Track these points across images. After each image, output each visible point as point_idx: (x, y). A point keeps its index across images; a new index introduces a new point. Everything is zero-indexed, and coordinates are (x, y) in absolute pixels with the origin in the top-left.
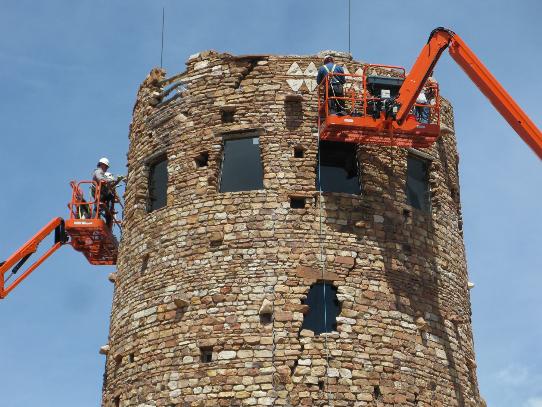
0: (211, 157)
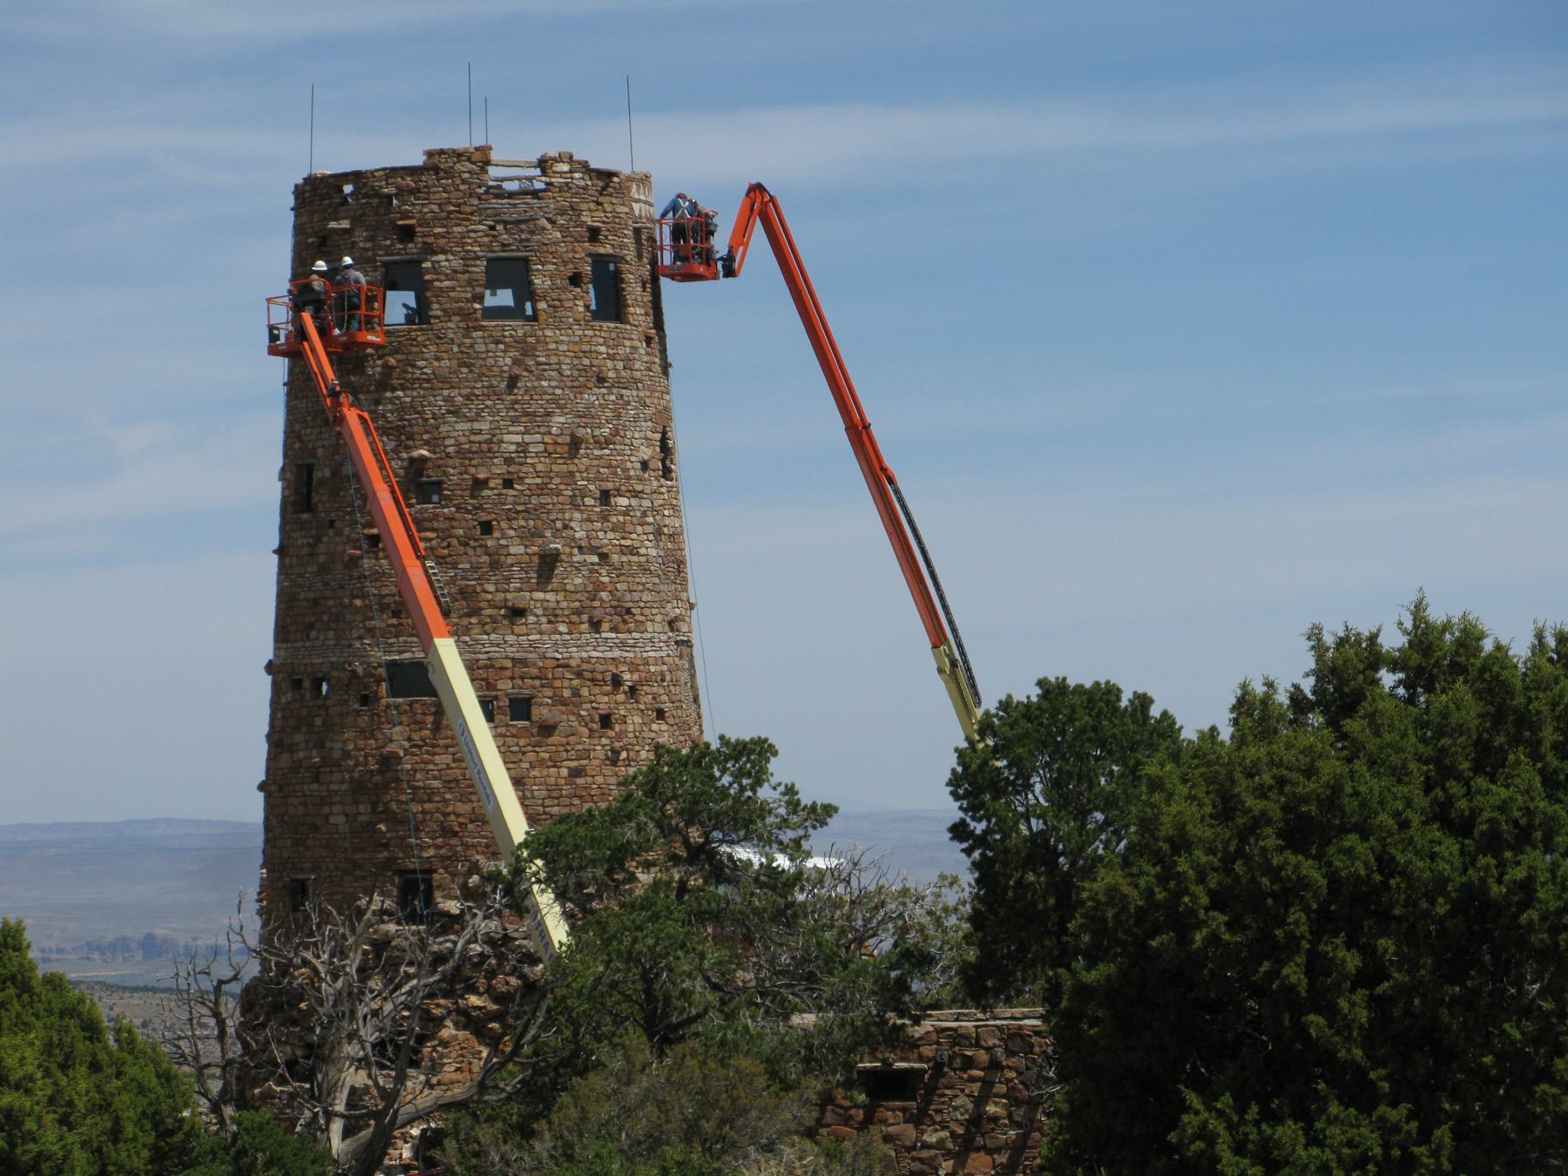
0: (586, 280)
